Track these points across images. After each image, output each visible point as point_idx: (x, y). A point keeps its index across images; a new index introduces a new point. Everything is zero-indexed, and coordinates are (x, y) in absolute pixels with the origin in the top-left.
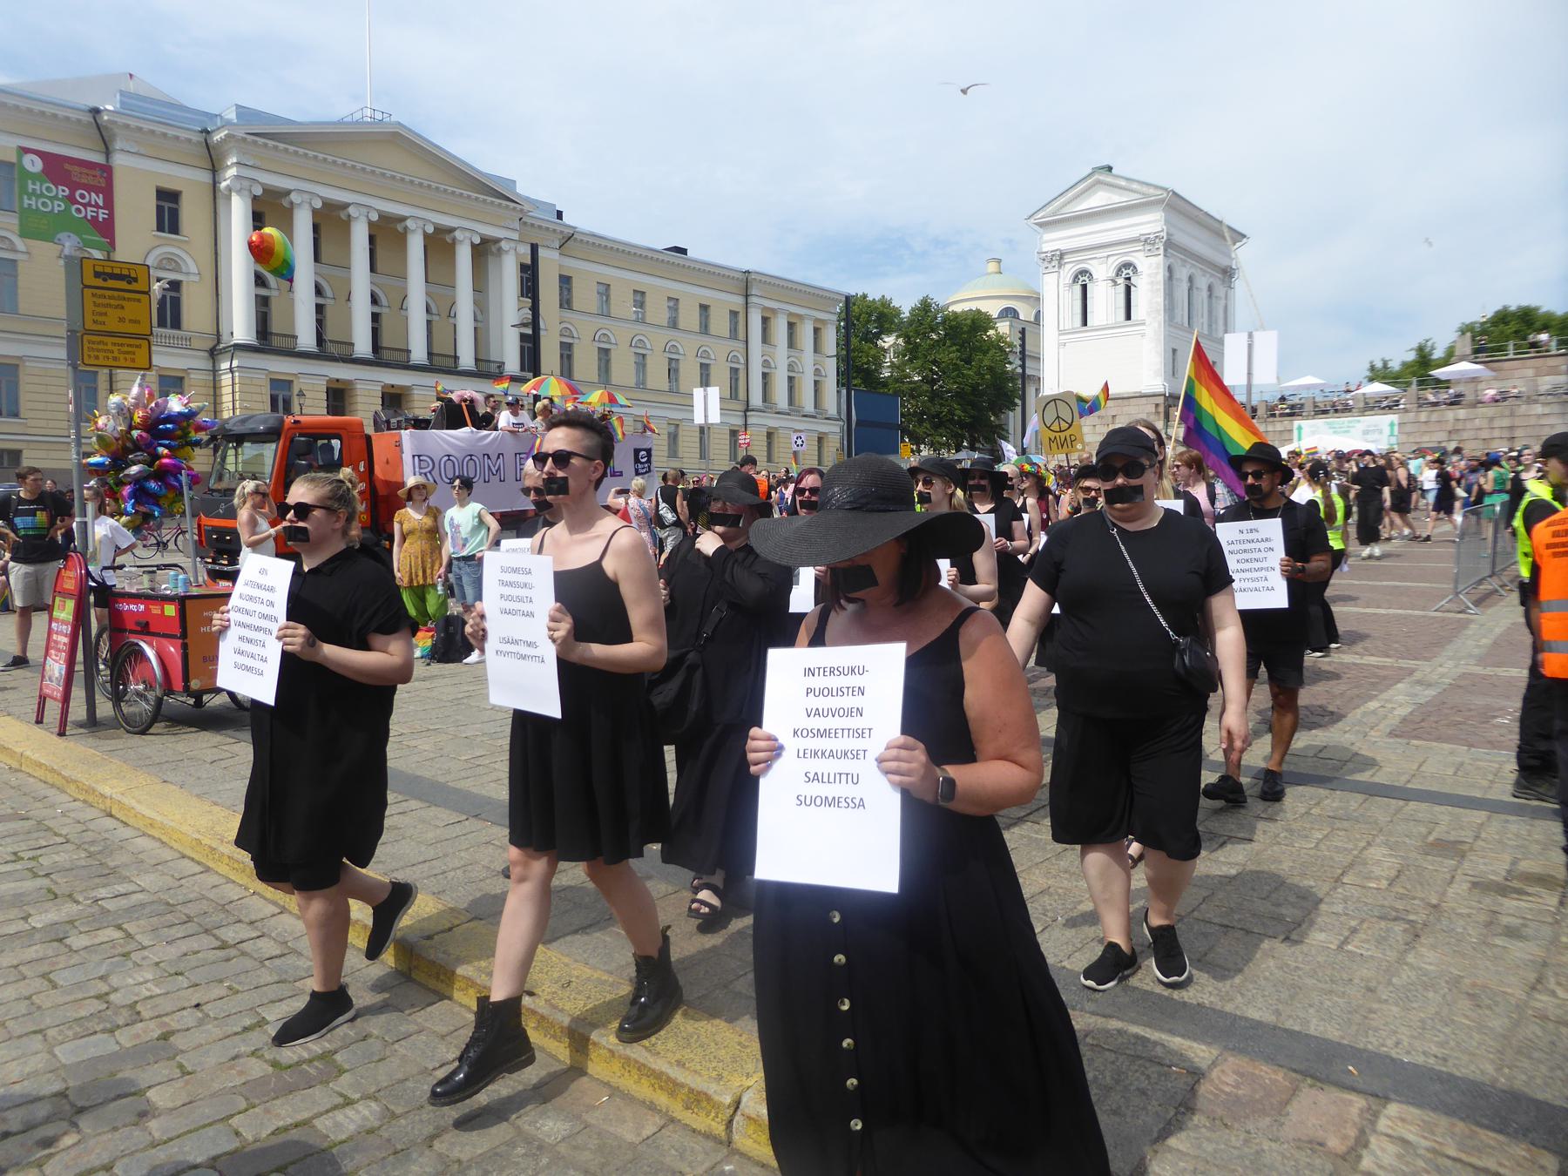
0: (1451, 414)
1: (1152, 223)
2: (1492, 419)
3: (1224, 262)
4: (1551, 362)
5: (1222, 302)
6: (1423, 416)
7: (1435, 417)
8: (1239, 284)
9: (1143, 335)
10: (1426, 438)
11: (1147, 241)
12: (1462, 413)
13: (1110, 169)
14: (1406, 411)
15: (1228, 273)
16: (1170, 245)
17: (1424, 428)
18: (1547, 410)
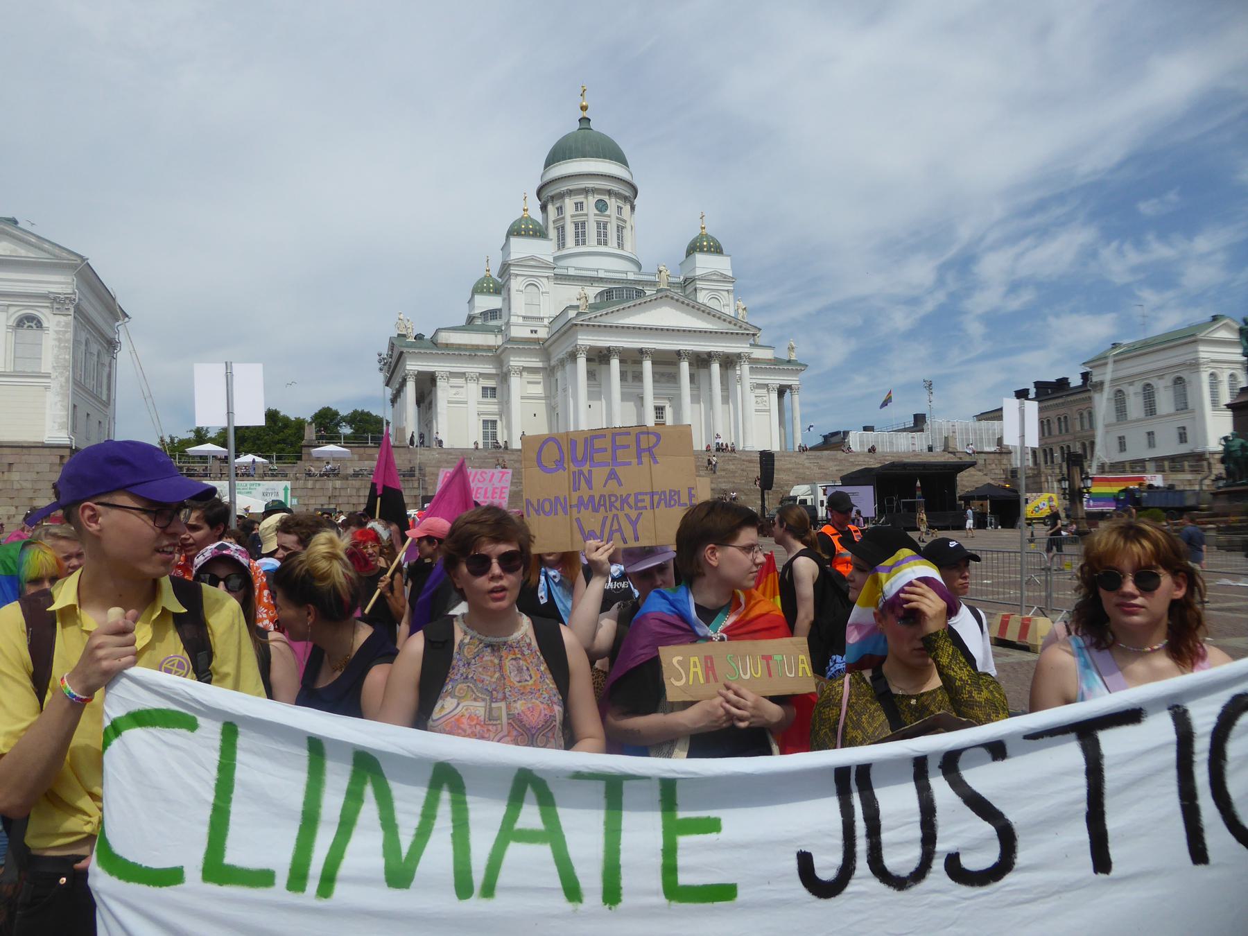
0: (330, 484)
1: (61, 284)
2: (358, 490)
3: (110, 334)
4: (369, 451)
5: (107, 369)
6: (310, 484)
7: (318, 485)
8: (123, 356)
9: (47, 388)
10: (312, 501)
11: (56, 302)
12: (338, 483)
13: (16, 222)
14: (297, 479)
15: (111, 345)
16: (78, 309)
17: (310, 493)
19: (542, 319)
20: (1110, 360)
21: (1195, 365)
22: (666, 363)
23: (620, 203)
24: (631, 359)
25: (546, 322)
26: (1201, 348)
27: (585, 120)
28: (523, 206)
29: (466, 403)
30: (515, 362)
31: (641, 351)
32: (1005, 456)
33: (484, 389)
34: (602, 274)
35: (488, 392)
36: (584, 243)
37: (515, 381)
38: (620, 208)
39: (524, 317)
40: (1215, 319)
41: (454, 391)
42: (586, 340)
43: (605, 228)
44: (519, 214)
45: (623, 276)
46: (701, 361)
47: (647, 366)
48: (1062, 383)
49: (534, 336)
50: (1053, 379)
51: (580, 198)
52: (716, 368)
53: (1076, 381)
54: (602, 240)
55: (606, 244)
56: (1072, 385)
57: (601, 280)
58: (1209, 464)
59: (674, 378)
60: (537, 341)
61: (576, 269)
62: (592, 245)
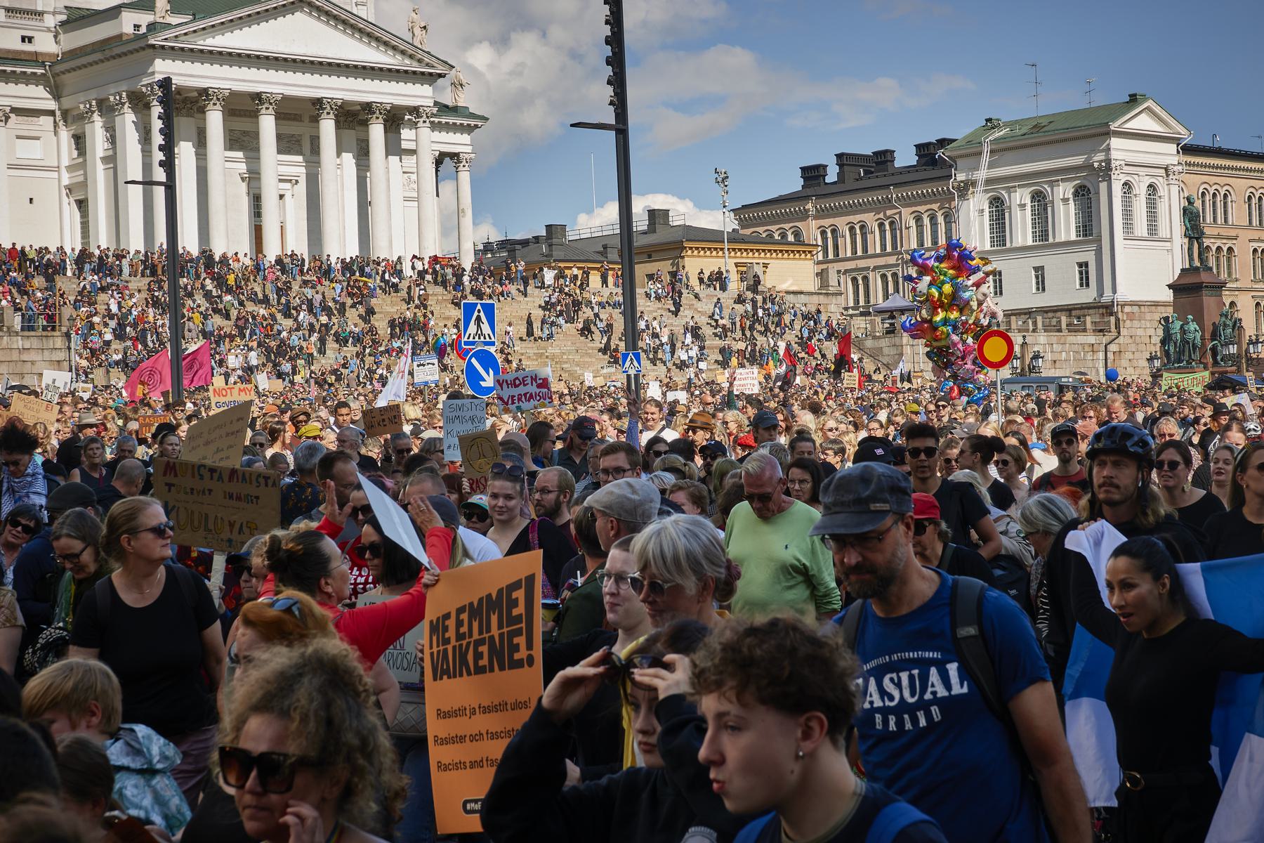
18: (27, 345)
19: (41, 14)
20: (986, 149)
21: (1106, 171)
22: (298, 120)
25: (50, 21)
26: (1115, 142)
31: (257, 96)
39: (8, 10)
40: (1134, 100)
46: (353, 118)
47: (268, 125)
48: (883, 158)
49: (27, 47)
50: (868, 151)
52: (377, 132)
53: (906, 158)
56: (898, 164)
58: (1118, 320)
60: (35, 59)
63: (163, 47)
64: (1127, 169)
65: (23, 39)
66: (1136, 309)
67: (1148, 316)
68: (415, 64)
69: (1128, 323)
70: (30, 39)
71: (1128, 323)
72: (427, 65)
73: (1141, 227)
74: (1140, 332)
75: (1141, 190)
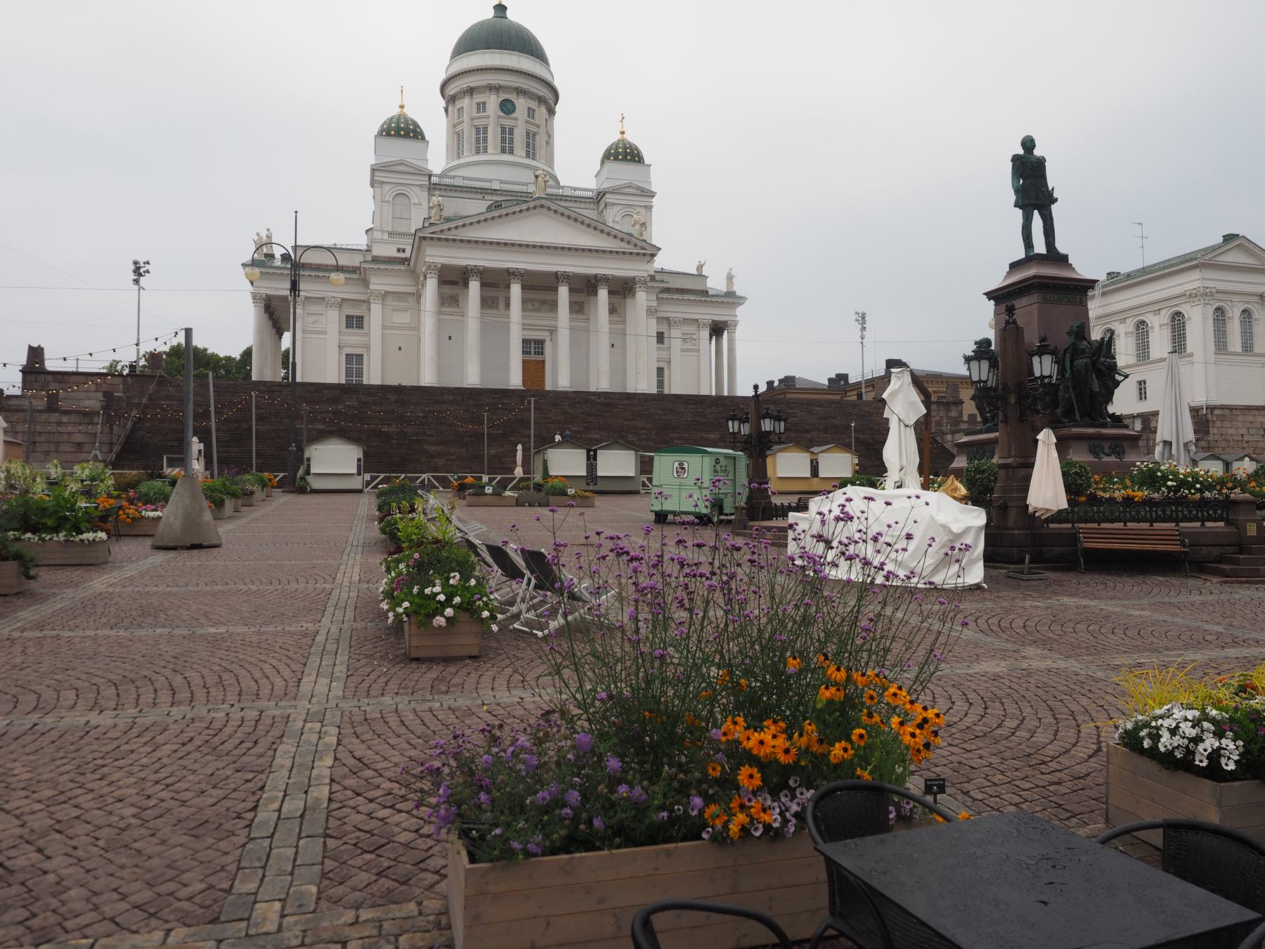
22: (540, 288)
23: (533, 104)
24: (495, 282)
27: (501, 9)
28: (399, 103)
29: (324, 333)
30: (378, 284)
32: (953, 408)
33: (349, 318)
34: (496, 186)
35: (355, 322)
36: (485, 151)
37: (376, 309)
38: (531, 112)
39: (390, 233)
41: (312, 319)
42: (437, 255)
43: (511, 132)
44: (395, 111)
45: (523, 188)
46: (585, 287)
47: (516, 290)
49: (401, 255)
51: (479, 98)
52: (603, 294)
54: (507, 146)
55: (511, 152)
57: (494, 192)
59: (554, 305)
61: (464, 178)
62: (493, 153)
63: (432, 239)
64: (1220, 296)
65: (399, 250)
66: (1227, 412)
67: (1240, 418)
68: (631, 246)
69: (1218, 424)
70: (404, 251)
71: (1218, 424)
72: (643, 249)
73: (1235, 344)
74: (1230, 431)
75: (1234, 313)
